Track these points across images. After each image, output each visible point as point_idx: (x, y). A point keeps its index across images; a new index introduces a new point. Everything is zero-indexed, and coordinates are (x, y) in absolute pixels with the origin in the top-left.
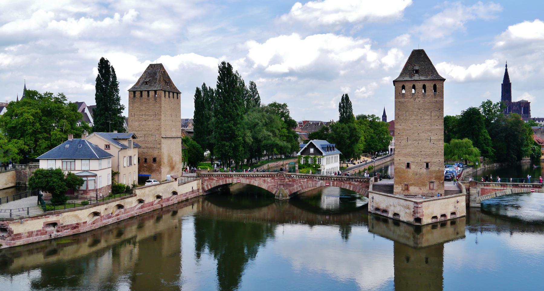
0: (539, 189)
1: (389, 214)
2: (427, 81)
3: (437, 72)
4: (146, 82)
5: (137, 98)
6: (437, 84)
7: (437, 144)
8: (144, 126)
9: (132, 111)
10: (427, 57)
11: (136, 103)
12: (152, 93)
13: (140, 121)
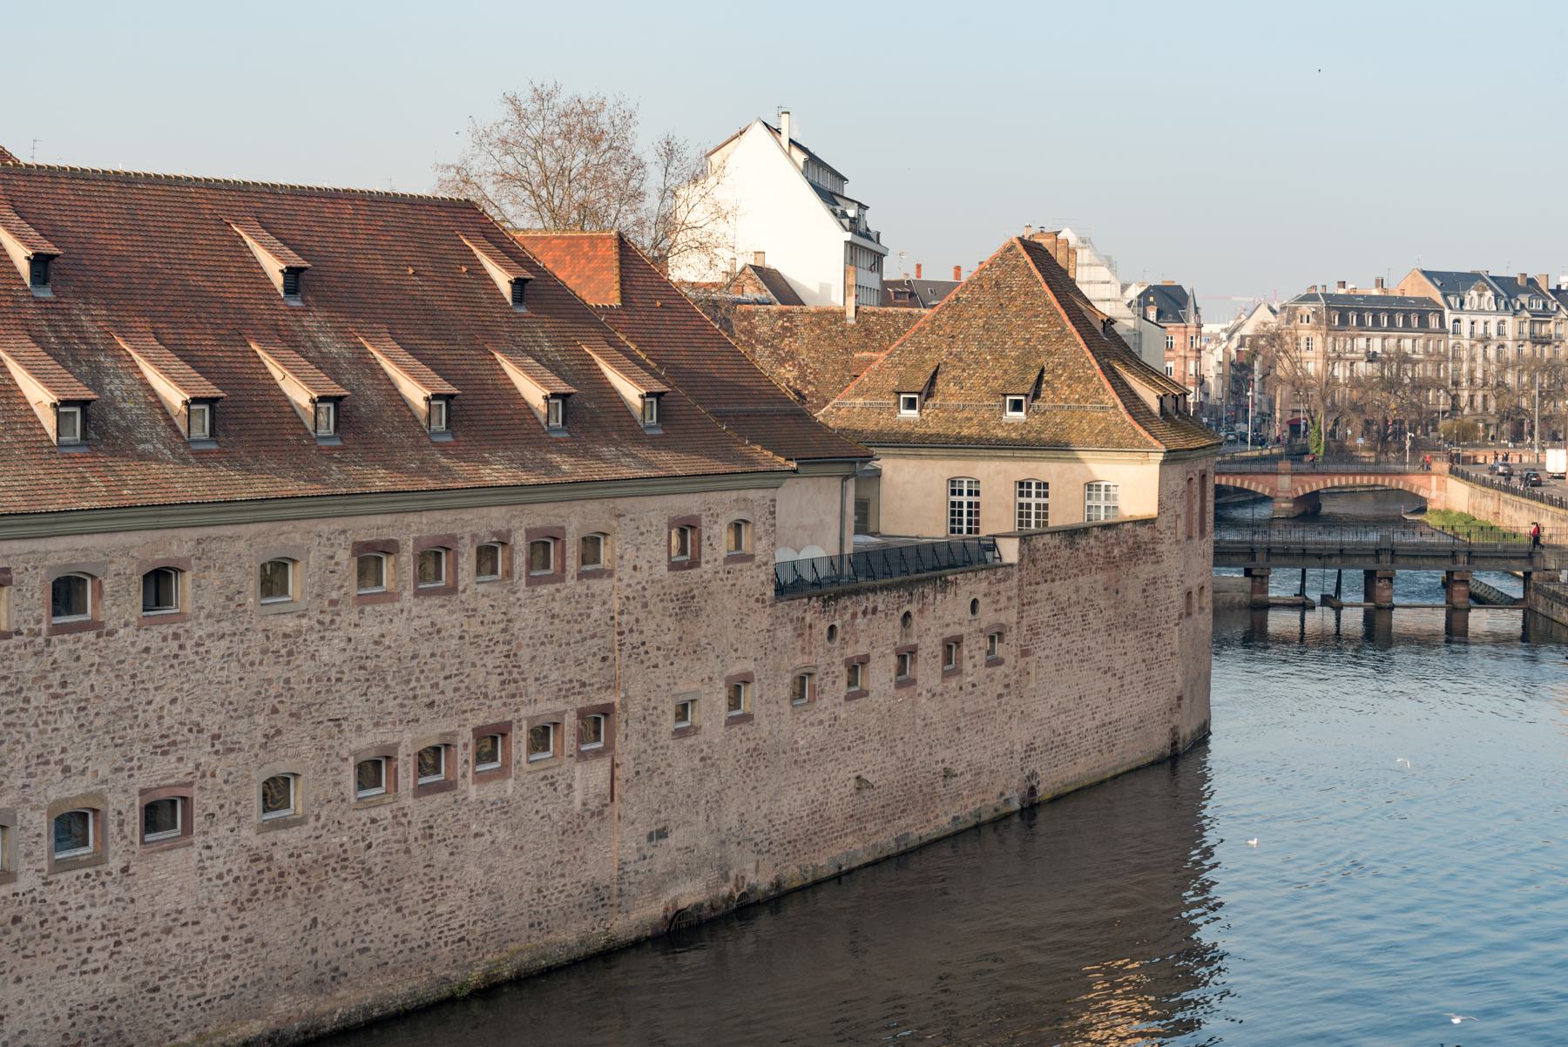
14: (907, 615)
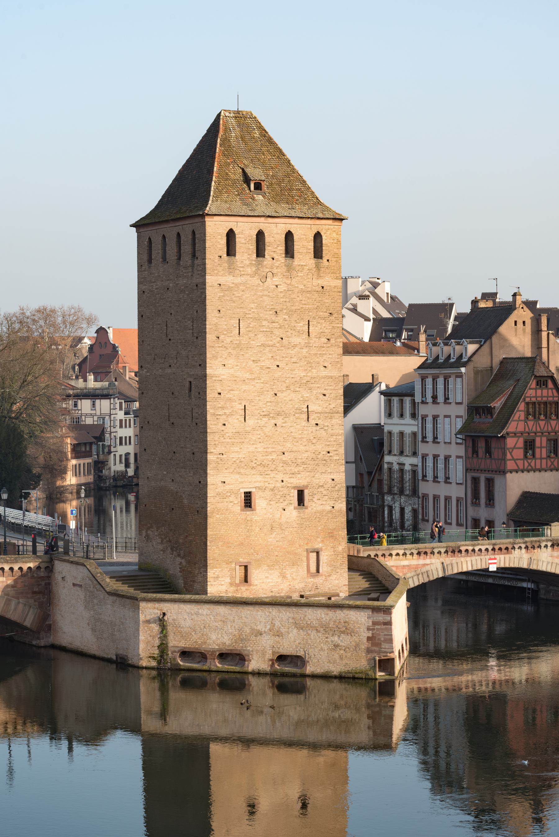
0: (507, 556)
1: (253, 662)
2: (297, 221)
3: (313, 193)
6: (322, 234)
7: (326, 428)
10: (270, 141)
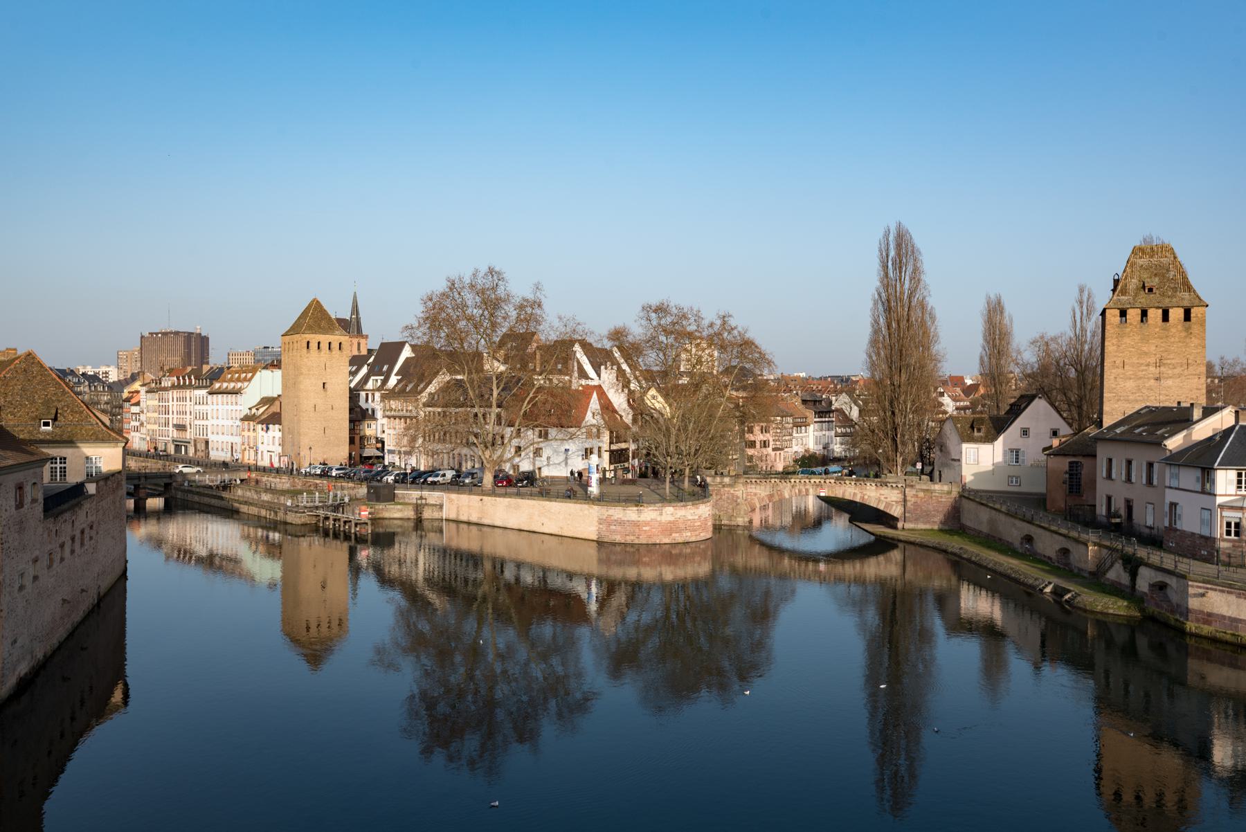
4: (1150, 290)
5: (1131, 324)
8: (1152, 390)
9: (1115, 354)
11: (1129, 337)
12: (1176, 314)
13: (1141, 378)
14: (73, 521)
